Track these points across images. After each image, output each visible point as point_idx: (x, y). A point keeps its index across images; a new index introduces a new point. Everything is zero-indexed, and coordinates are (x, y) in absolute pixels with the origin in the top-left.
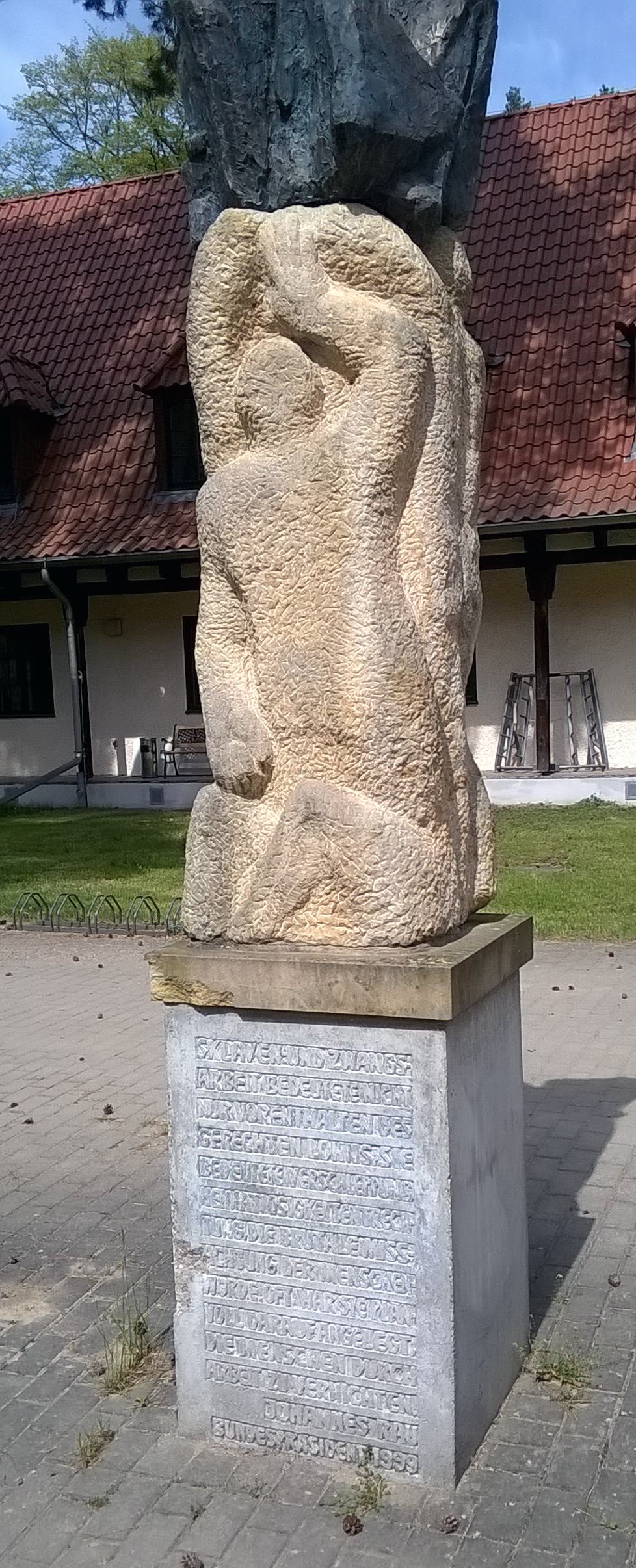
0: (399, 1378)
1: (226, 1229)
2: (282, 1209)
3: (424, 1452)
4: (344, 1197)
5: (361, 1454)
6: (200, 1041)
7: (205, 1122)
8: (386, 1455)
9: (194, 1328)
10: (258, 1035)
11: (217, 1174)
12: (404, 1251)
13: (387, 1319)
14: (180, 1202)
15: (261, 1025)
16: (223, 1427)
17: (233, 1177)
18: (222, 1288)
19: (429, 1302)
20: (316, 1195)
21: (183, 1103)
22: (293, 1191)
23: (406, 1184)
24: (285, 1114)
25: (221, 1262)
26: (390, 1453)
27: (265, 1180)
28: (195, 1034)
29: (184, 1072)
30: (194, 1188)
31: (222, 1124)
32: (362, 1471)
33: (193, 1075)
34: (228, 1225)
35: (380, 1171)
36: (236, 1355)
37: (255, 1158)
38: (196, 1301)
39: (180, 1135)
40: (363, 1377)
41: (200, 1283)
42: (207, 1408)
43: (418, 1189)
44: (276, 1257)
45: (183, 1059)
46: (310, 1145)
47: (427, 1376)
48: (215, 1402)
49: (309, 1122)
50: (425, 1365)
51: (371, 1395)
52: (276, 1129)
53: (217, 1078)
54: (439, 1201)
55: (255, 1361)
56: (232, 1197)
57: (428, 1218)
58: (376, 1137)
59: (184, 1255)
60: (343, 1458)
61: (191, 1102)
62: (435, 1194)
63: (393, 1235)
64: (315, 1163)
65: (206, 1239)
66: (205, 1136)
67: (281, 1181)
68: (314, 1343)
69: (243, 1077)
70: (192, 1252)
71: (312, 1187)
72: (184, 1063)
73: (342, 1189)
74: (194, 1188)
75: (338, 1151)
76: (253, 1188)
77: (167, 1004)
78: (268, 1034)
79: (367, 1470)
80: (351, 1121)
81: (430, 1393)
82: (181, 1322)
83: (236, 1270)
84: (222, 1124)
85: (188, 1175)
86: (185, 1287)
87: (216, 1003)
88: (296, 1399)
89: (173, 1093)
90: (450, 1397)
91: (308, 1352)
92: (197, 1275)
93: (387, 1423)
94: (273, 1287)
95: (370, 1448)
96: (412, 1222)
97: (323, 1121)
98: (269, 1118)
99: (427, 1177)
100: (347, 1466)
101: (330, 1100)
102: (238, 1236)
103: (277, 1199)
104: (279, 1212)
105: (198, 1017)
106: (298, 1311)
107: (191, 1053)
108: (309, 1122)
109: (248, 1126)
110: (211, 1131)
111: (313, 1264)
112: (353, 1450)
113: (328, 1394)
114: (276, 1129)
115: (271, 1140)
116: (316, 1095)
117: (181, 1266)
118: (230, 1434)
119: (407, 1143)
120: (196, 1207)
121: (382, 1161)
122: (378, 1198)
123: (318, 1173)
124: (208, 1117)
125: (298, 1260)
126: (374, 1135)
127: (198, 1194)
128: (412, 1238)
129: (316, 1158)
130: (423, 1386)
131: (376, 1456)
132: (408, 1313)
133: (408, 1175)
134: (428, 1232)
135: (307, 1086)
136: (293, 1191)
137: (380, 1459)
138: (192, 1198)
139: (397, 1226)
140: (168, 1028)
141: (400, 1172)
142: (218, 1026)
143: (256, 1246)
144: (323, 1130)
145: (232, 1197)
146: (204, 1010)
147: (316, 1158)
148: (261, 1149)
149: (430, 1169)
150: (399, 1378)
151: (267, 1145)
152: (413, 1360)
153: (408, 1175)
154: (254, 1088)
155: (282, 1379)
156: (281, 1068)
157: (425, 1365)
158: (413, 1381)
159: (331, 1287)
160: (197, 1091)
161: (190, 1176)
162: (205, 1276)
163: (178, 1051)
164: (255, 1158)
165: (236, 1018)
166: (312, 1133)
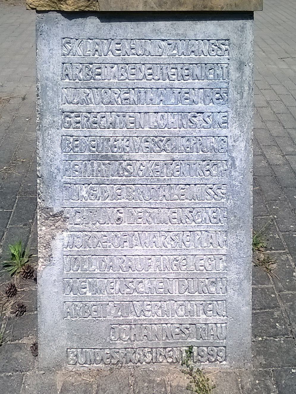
0: (213, 289)
1: (84, 193)
2: (128, 171)
3: (231, 343)
4: (176, 156)
5: (184, 354)
6: (67, 41)
7: (67, 107)
8: (203, 351)
9: (54, 278)
10: (112, 33)
11: (76, 149)
12: (219, 191)
13: (205, 245)
14: (45, 175)
15: (115, 25)
16: (76, 356)
17: (90, 150)
18: (78, 242)
19: (236, 227)
20: (154, 156)
21: (50, 93)
22: (137, 156)
23: (224, 139)
24: (133, 96)
25: (78, 220)
26: (205, 349)
27: (115, 150)
28: (62, 35)
29: (52, 66)
30: (58, 163)
31: (82, 108)
32: (185, 368)
33: (58, 70)
34: (85, 190)
35: (204, 132)
36: (89, 294)
37: (107, 133)
38: (57, 255)
39: (48, 119)
40: (186, 293)
41: (61, 242)
42: (63, 343)
43: (230, 142)
44: (122, 210)
45: (50, 57)
46: (153, 118)
47: (234, 284)
48: (70, 336)
49: (151, 100)
50: (232, 276)
51: (192, 306)
52: (125, 108)
53: (78, 70)
54: (246, 149)
55: (104, 296)
56: (89, 166)
57: (237, 163)
58: (200, 106)
59: (47, 219)
60: (170, 360)
61: (56, 93)
62: (243, 145)
63: (212, 180)
64: (155, 132)
65: (67, 204)
66: (68, 119)
67: (128, 149)
68: (151, 273)
69: (100, 68)
70: (54, 216)
71: (152, 150)
72: (51, 60)
73: (175, 149)
74: (58, 163)
75: (173, 120)
76: (106, 157)
77: (38, 12)
78: (121, 32)
79: (188, 366)
80: (184, 95)
81: (236, 297)
82: (44, 274)
83: (90, 225)
84: (82, 108)
85: (53, 153)
86: (48, 245)
87: (82, 8)
88: (135, 320)
89: (42, 85)
90: (249, 297)
91: (146, 281)
92: (58, 236)
93: (204, 326)
94: (119, 234)
95: (191, 348)
96: (226, 167)
97: (162, 98)
98: (119, 100)
99: (237, 132)
100: (172, 368)
101: (167, 81)
102: (92, 197)
103: (124, 164)
104: (126, 173)
105: (65, 22)
106: (139, 250)
107: (58, 51)
108: (151, 100)
109: (104, 108)
110: (73, 115)
111: (151, 211)
112: (177, 353)
113: (160, 312)
114: (125, 108)
115: (121, 117)
116: (156, 78)
117: (44, 228)
118: (82, 360)
119: (224, 108)
120: (59, 178)
121: (204, 124)
122: (201, 153)
123: (157, 140)
124: (70, 103)
125: (139, 210)
126: (200, 105)
127: (61, 167)
128: (225, 180)
129: (155, 127)
130: (231, 292)
131: (195, 354)
132: (221, 238)
133: (224, 132)
134: (237, 174)
135: (150, 71)
136: (137, 156)
137: (198, 354)
138: (56, 171)
139: (214, 173)
140: (39, 32)
141: (217, 131)
142: (81, 28)
143: (107, 203)
144: (161, 105)
145: (89, 166)
146: (70, 15)
147: (155, 127)
148: (113, 125)
149: (240, 126)
150: (213, 289)
151: (118, 121)
152: (224, 274)
153: (224, 132)
154: (109, 76)
155: (124, 307)
156: (132, 58)
157: (232, 276)
158: (224, 290)
159: (165, 227)
160: (61, 83)
161: (54, 153)
162: (65, 234)
163: (47, 50)
164: (107, 133)
165: (95, 21)
166: (153, 108)
